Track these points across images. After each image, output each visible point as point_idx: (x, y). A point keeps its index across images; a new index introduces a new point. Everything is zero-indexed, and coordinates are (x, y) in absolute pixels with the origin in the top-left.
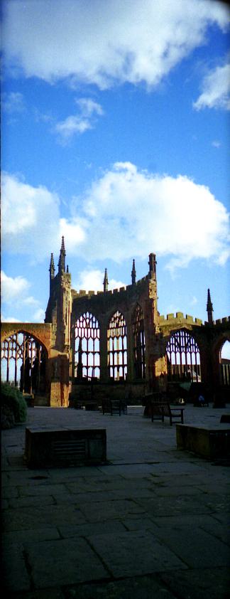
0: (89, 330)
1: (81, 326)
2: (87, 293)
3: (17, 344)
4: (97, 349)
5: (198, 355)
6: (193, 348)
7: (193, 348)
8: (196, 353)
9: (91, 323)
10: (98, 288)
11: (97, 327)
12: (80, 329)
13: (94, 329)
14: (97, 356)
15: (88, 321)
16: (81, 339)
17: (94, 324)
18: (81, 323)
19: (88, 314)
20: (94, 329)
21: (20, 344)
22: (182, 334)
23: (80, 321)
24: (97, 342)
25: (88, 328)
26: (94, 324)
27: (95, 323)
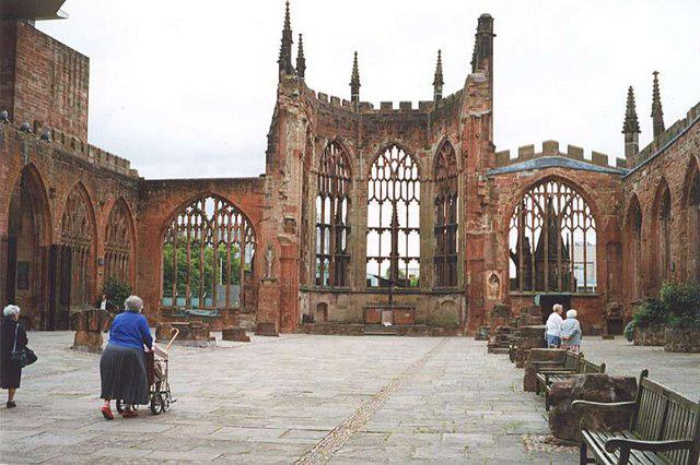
0: (398, 183)
1: (381, 177)
2: (396, 106)
3: (204, 218)
4: (415, 222)
5: (592, 237)
6: (578, 220)
7: (578, 220)
8: (585, 230)
9: (401, 169)
10: (419, 92)
11: (415, 177)
12: (378, 183)
13: (408, 182)
14: (414, 236)
15: (395, 165)
16: (394, 203)
17: (408, 170)
18: (381, 170)
19: (395, 150)
20: (408, 182)
21: (209, 218)
22: (552, 188)
23: (378, 168)
24: (415, 208)
25: (394, 177)
26: (408, 170)
27: (411, 168)
